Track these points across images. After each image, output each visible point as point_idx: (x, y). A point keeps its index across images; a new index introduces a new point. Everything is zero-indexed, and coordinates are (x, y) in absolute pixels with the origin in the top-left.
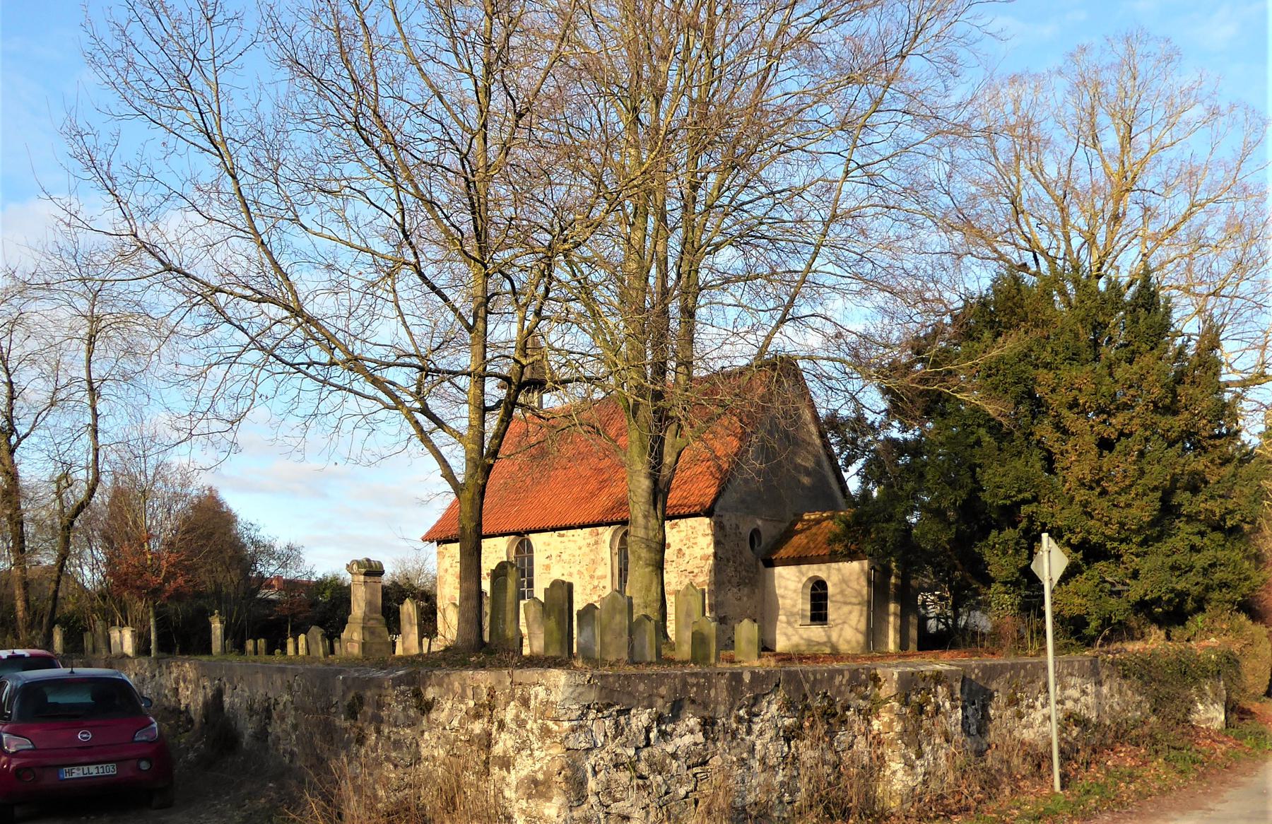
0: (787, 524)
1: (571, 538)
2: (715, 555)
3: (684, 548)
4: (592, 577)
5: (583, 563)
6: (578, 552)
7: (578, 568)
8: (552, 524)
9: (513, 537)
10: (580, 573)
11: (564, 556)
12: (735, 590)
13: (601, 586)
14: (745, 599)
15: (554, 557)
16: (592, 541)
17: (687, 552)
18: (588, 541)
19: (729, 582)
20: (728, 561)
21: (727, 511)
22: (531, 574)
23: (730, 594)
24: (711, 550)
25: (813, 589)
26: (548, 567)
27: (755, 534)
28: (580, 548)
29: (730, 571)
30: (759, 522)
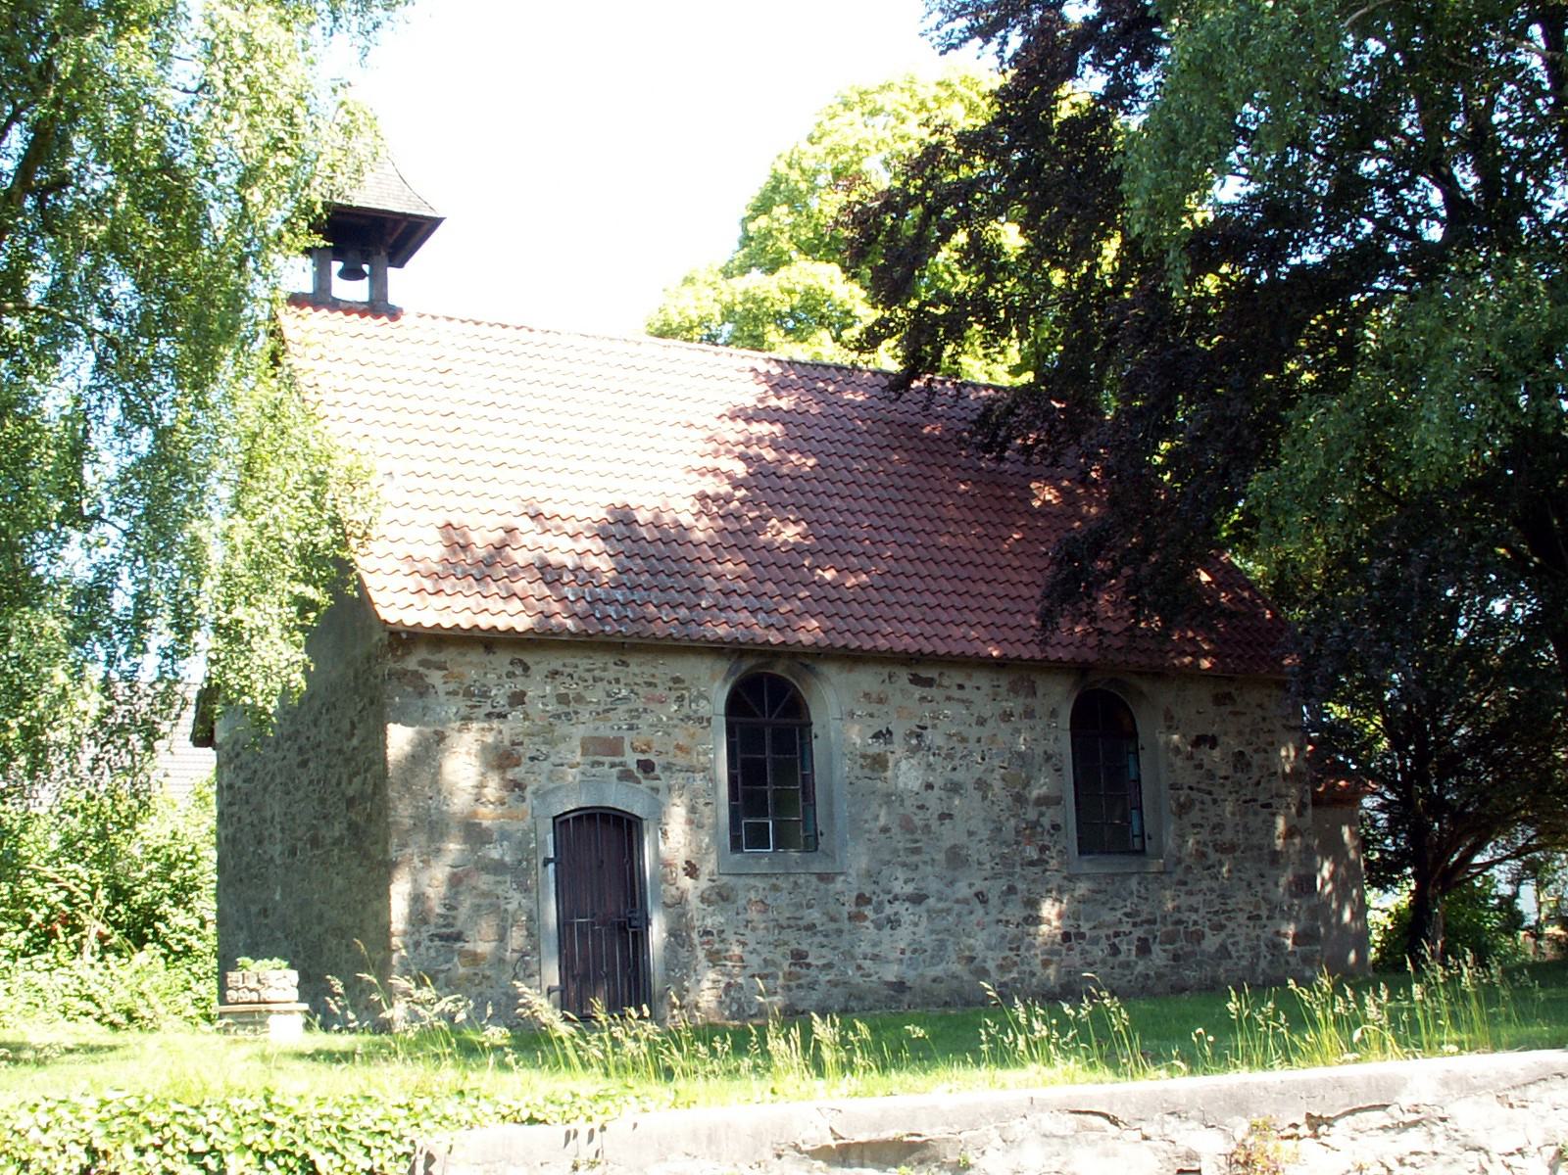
3: (1248, 751)
4: (1020, 799)
6: (975, 732)
7: (978, 771)
10: (982, 785)
13: (1046, 821)
15: (898, 737)
18: (1008, 705)
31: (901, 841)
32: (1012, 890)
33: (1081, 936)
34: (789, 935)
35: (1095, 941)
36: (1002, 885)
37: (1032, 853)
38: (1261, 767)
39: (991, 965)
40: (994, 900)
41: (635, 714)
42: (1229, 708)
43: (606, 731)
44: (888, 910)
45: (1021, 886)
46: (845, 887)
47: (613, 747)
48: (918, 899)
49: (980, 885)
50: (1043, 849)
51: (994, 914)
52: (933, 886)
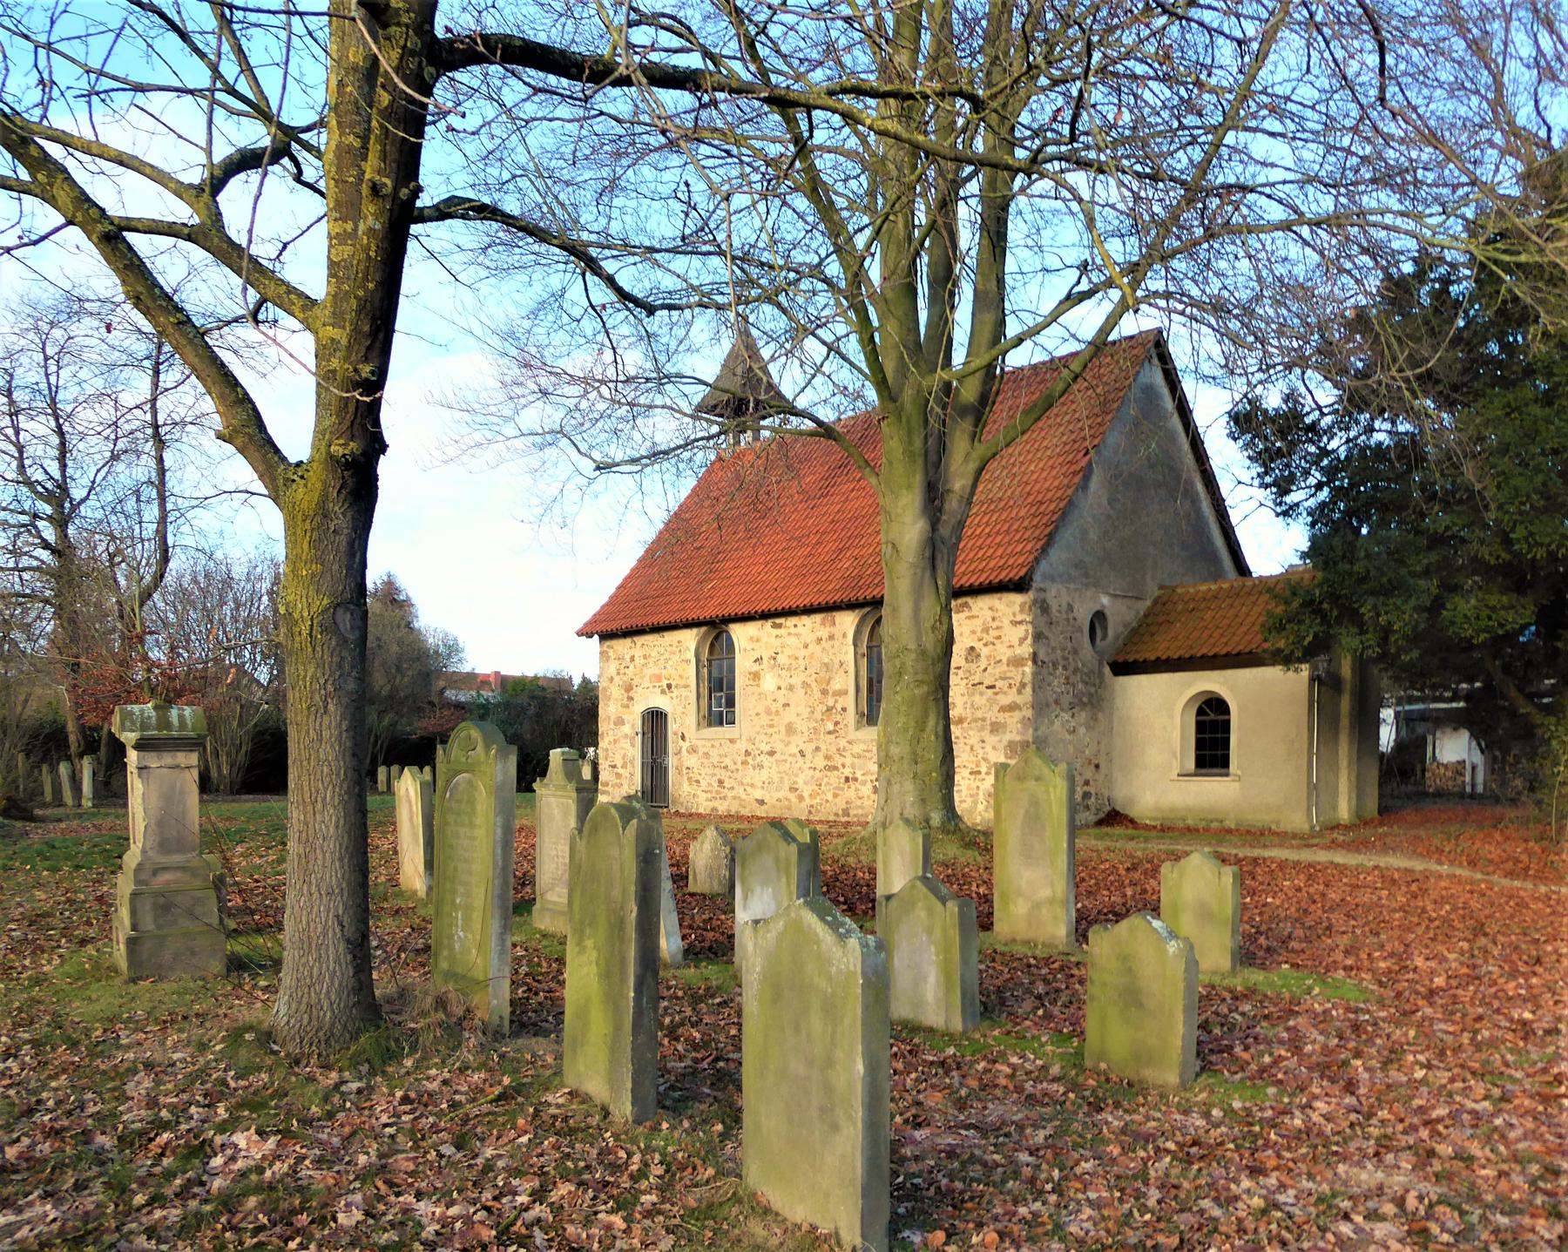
0: (1148, 603)
1: (793, 630)
2: (1034, 657)
4: (824, 692)
5: (811, 671)
6: (803, 652)
7: (803, 677)
8: (763, 606)
9: (703, 629)
10: (806, 685)
11: (782, 659)
12: (1066, 716)
13: (839, 707)
14: (1082, 730)
16: (823, 632)
17: (985, 651)
18: (819, 634)
19: (1057, 702)
20: (1055, 665)
21: (1052, 579)
22: (732, 687)
23: (1057, 723)
24: (1026, 650)
25: (1200, 712)
26: (756, 676)
27: (1099, 617)
28: (806, 646)
29: (1058, 683)
30: (1105, 600)
31: (765, 720)
32: (818, 749)
33: (856, 779)
34: (717, 771)
35: (864, 783)
36: (812, 746)
37: (830, 727)
38: (988, 657)
39: (806, 795)
40: (809, 755)
41: (666, 660)
42: (966, 614)
43: (657, 672)
44: (759, 759)
45: (823, 747)
46: (742, 745)
47: (658, 678)
48: (772, 753)
49: (802, 746)
50: (837, 723)
51: (808, 764)
52: (779, 747)
